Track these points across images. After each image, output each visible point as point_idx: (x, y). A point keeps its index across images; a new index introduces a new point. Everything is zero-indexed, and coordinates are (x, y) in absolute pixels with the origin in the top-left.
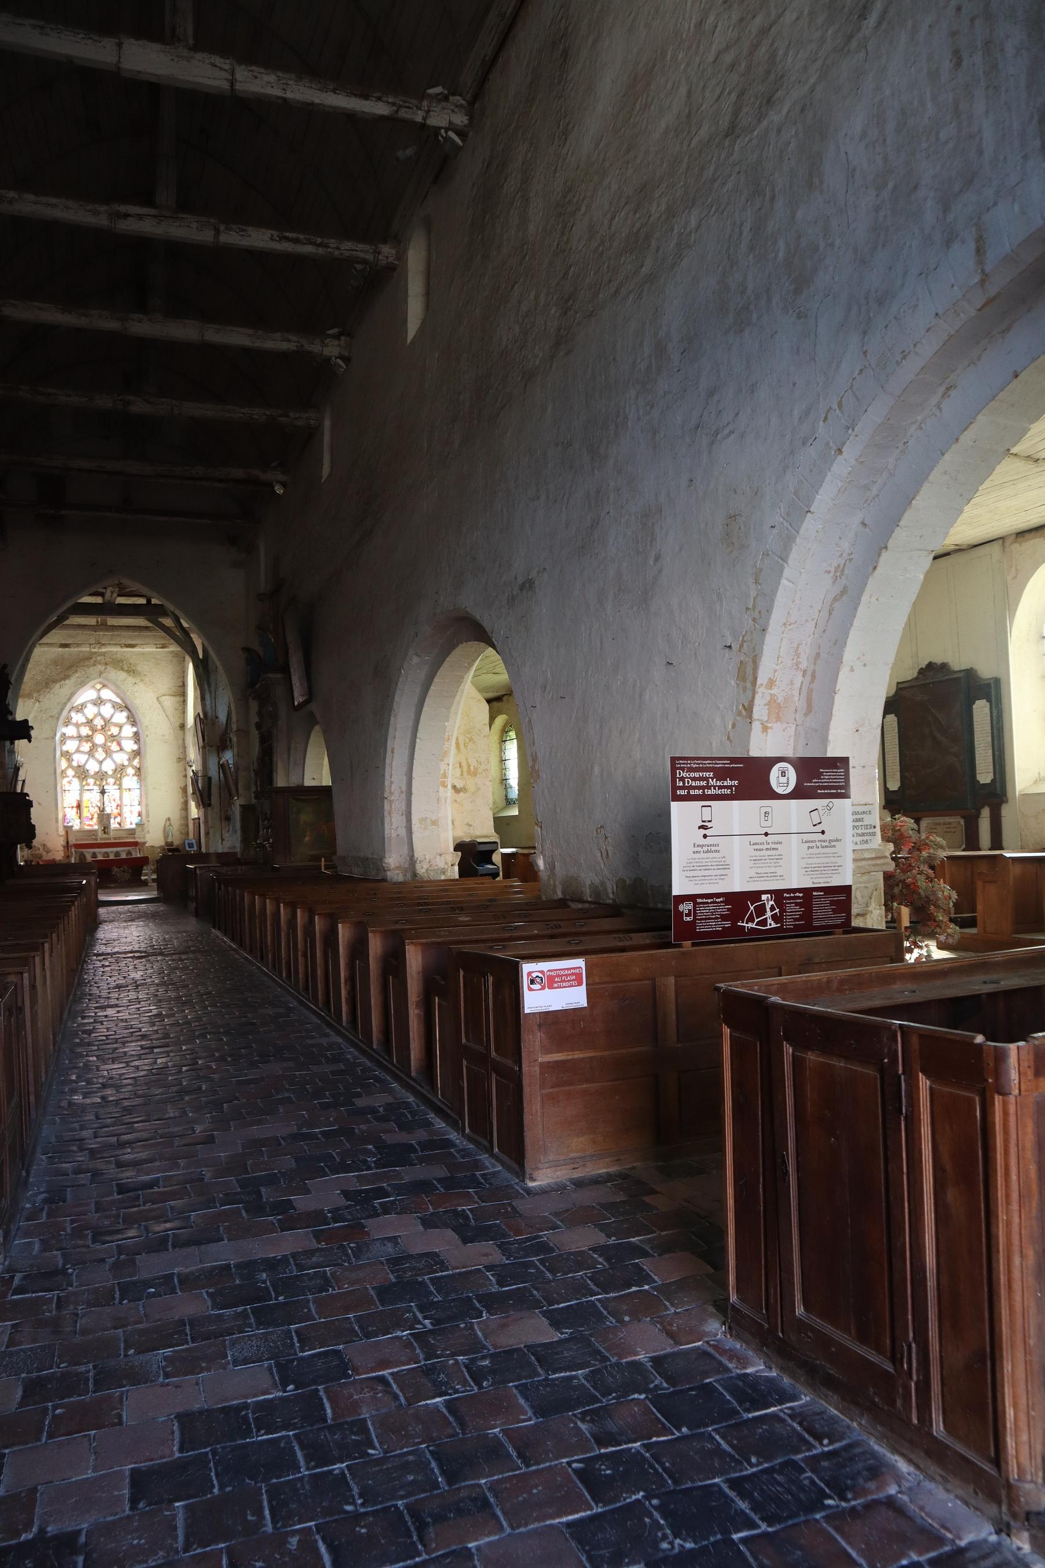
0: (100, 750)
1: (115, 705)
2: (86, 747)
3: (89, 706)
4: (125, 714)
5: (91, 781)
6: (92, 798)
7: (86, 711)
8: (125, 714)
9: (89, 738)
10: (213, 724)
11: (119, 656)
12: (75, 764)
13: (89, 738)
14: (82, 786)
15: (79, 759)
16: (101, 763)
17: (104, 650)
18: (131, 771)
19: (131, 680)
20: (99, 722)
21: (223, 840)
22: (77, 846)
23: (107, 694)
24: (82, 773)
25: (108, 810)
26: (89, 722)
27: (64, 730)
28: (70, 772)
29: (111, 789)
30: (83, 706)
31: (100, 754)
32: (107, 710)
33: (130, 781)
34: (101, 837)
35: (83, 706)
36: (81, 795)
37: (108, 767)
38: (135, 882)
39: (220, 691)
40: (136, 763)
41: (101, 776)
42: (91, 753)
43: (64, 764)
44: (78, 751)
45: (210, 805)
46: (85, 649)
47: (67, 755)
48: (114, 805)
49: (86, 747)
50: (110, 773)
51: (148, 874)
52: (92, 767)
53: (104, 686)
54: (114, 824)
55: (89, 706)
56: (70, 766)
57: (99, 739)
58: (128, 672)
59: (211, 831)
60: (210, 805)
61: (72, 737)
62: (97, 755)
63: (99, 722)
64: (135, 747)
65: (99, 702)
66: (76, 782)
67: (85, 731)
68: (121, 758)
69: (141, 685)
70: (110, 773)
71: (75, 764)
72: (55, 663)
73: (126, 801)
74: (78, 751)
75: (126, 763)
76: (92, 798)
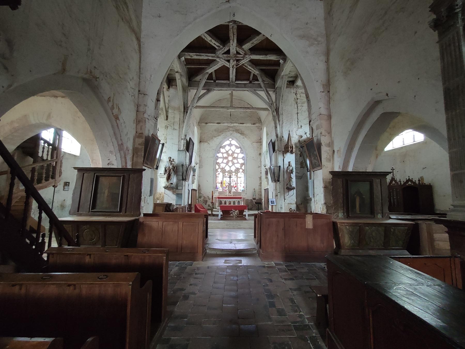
0: (230, 162)
1: (236, 146)
2: (225, 161)
3: (227, 146)
4: (239, 149)
5: (227, 174)
6: (227, 180)
7: (226, 148)
8: (239, 149)
9: (226, 158)
10: (281, 140)
11: (238, 128)
12: (221, 167)
13: (226, 158)
14: (223, 175)
15: (223, 165)
16: (230, 167)
17: (232, 125)
18: (241, 170)
19: (242, 136)
20: (230, 152)
21: (285, 199)
22: (219, 198)
23: (234, 142)
24: (223, 171)
25: (232, 185)
26: (227, 152)
27: (218, 155)
28: (219, 170)
29: (234, 178)
30: (225, 146)
31: (230, 164)
32: (233, 148)
33: (241, 175)
34: (227, 194)
35: (225, 146)
36: (223, 179)
37: (233, 169)
38: (241, 216)
39: (284, 124)
40: (243, 168)
41: (230, 172)
42: (227, 163)
43: (217, 167)
44: (222, 162)
45: (279, 181)
46: (226, 124)
47: (218, 164)
48: (234, 183)
49: (225, 161)
50: (233, 171)
51: (246, 213)
52: (227, 169)
53: (232, 139)
54: (233, 190)
55: (227, 146)
56: (219, 168)
57: (230, 158)
58: (241, 134)
59: (279, 194)
60: (279, 181)
61: (221, 158)
62: (229, 164)
63: (230, 152)
64: (243, 162)
65: (230, 145)
66: (221, 174)
67: (225, 155)
68: (238, 166)
69: (245, 139)
70: (233, 171)
71: (221, 167)
72: (215, 130)
73: (239, 182)
74: (222, 162)
75: (239, 167)
76: (227, 180)
